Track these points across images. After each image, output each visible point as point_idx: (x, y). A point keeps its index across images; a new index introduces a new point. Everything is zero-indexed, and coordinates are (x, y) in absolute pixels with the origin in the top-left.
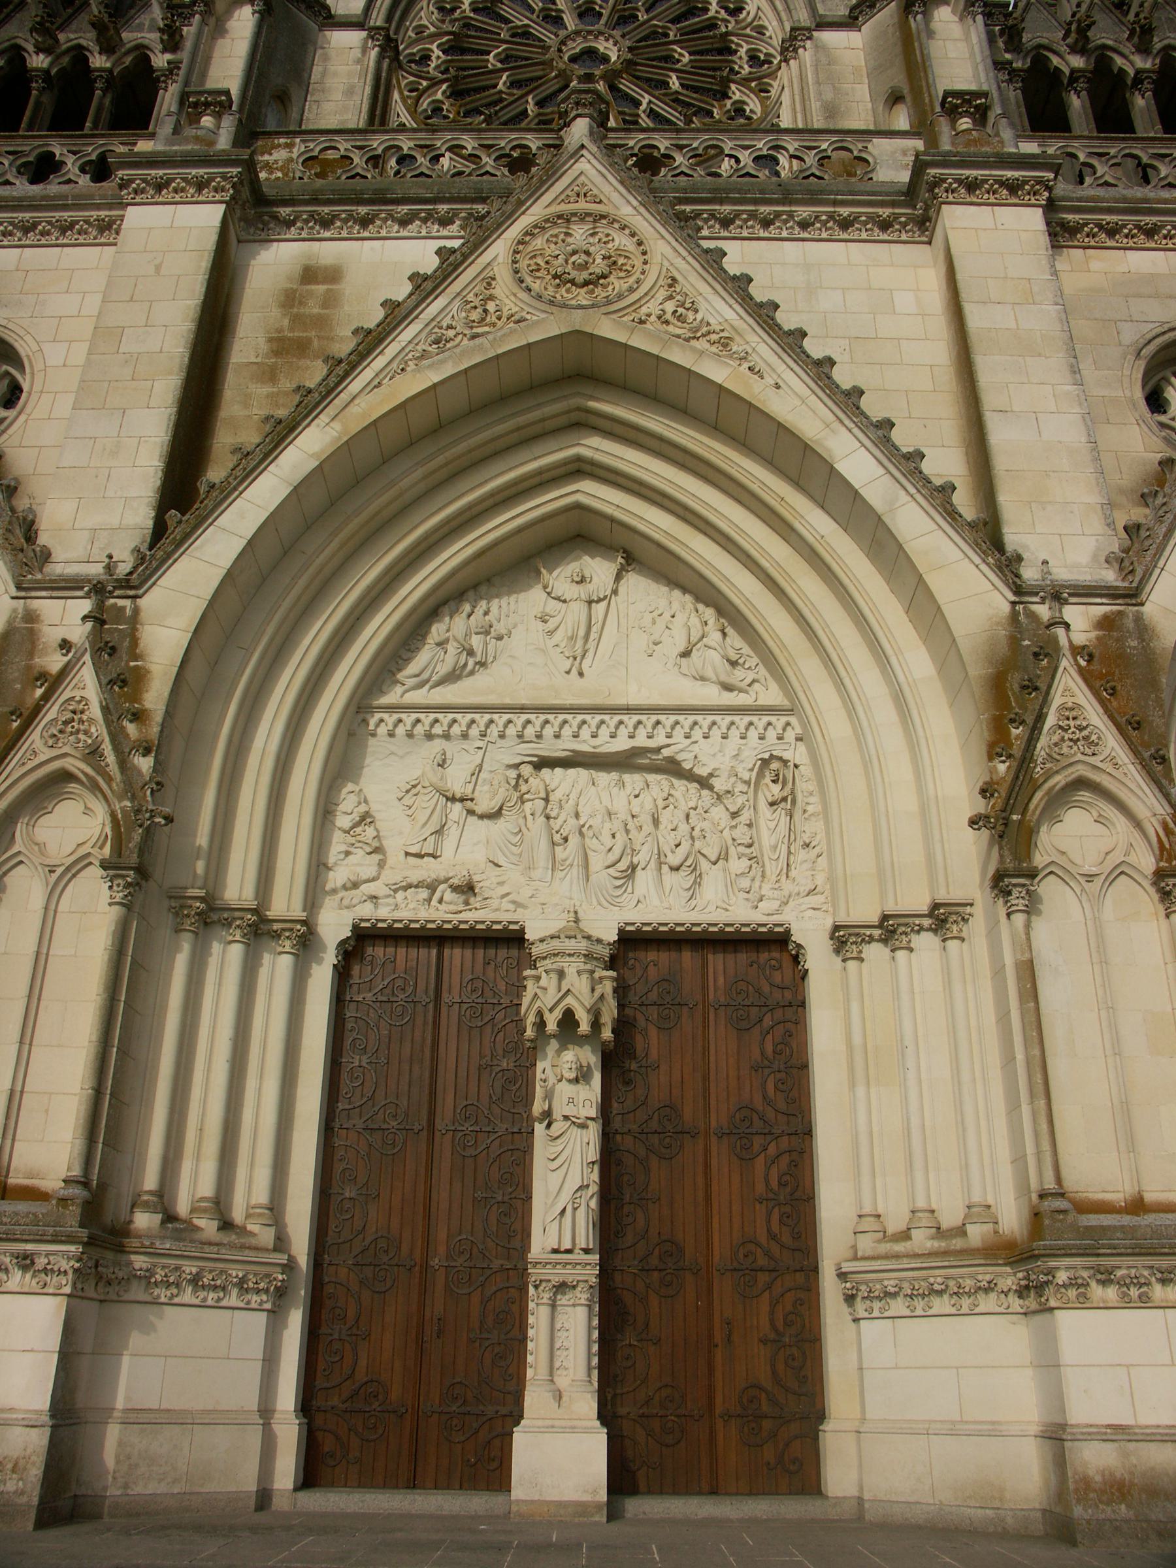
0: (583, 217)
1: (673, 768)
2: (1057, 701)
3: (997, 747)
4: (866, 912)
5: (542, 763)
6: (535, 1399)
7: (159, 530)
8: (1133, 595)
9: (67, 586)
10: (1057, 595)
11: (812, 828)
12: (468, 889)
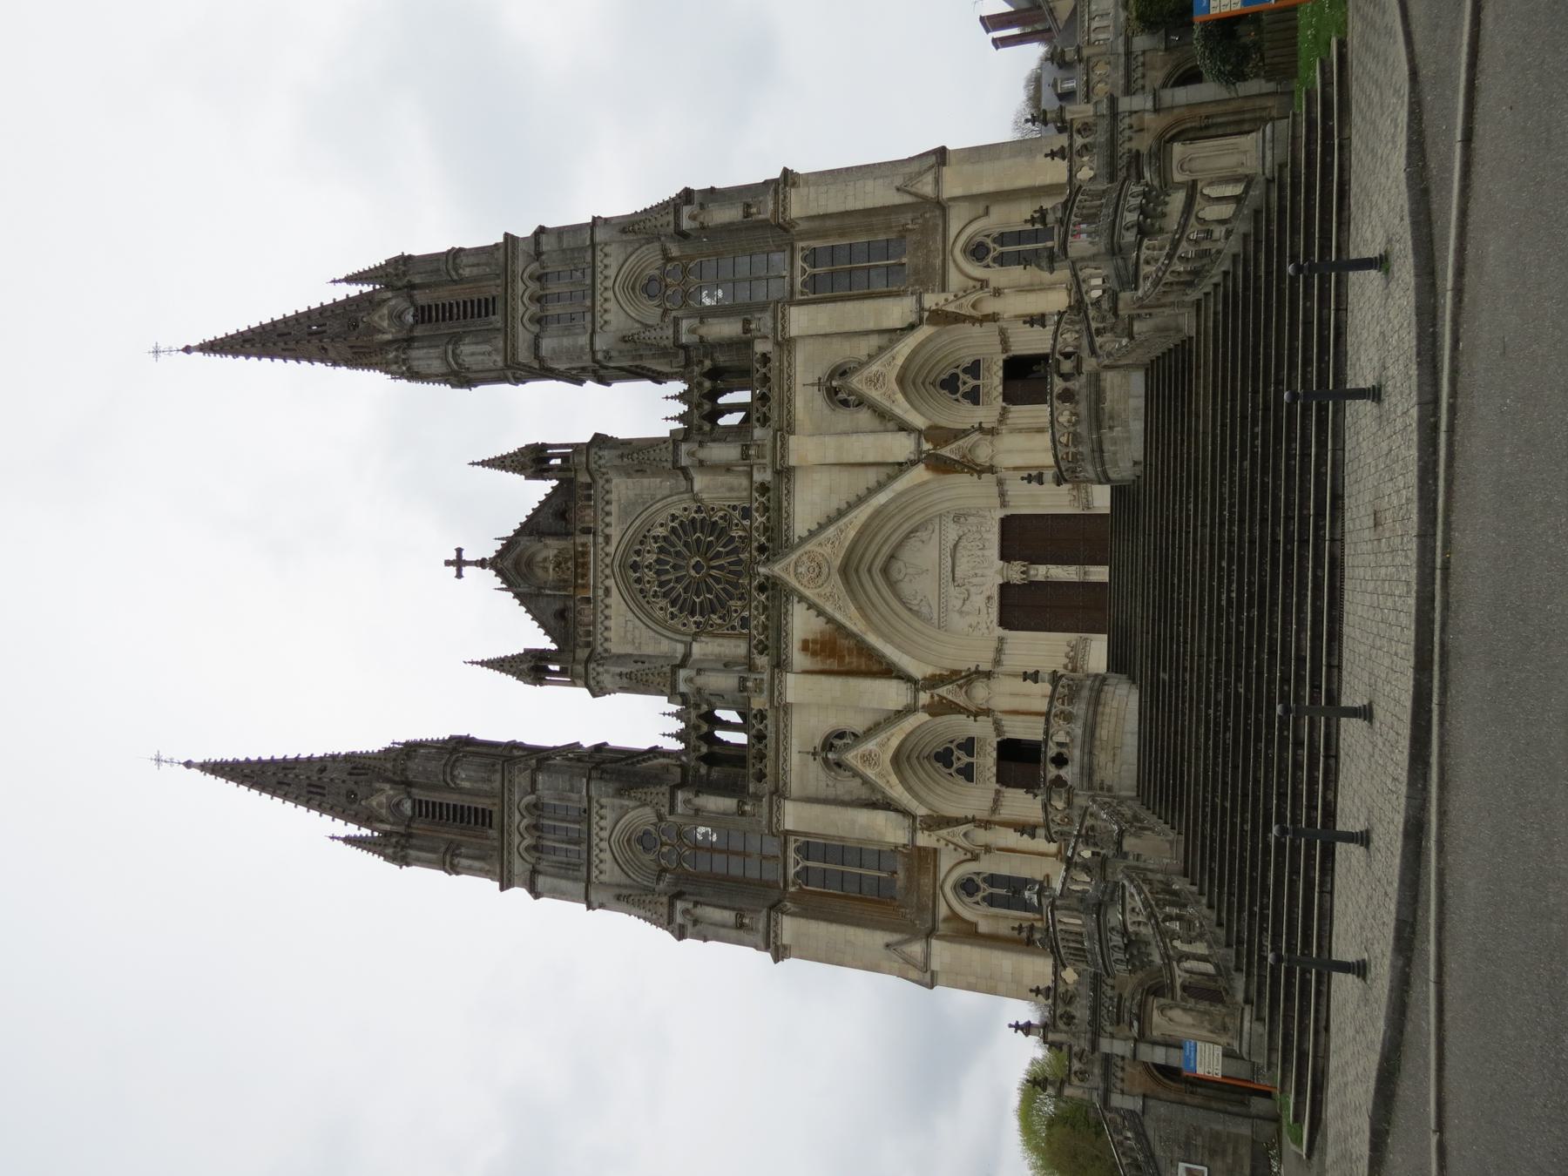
0: (795, 570)
1: (955, 546)
2: (948, 455)
4: (997, 501)
5: (953, 580)
8: (920, 432)
9: (916, 698)
10: (921, 452)
11: (974, 512)
12: (989, 598)
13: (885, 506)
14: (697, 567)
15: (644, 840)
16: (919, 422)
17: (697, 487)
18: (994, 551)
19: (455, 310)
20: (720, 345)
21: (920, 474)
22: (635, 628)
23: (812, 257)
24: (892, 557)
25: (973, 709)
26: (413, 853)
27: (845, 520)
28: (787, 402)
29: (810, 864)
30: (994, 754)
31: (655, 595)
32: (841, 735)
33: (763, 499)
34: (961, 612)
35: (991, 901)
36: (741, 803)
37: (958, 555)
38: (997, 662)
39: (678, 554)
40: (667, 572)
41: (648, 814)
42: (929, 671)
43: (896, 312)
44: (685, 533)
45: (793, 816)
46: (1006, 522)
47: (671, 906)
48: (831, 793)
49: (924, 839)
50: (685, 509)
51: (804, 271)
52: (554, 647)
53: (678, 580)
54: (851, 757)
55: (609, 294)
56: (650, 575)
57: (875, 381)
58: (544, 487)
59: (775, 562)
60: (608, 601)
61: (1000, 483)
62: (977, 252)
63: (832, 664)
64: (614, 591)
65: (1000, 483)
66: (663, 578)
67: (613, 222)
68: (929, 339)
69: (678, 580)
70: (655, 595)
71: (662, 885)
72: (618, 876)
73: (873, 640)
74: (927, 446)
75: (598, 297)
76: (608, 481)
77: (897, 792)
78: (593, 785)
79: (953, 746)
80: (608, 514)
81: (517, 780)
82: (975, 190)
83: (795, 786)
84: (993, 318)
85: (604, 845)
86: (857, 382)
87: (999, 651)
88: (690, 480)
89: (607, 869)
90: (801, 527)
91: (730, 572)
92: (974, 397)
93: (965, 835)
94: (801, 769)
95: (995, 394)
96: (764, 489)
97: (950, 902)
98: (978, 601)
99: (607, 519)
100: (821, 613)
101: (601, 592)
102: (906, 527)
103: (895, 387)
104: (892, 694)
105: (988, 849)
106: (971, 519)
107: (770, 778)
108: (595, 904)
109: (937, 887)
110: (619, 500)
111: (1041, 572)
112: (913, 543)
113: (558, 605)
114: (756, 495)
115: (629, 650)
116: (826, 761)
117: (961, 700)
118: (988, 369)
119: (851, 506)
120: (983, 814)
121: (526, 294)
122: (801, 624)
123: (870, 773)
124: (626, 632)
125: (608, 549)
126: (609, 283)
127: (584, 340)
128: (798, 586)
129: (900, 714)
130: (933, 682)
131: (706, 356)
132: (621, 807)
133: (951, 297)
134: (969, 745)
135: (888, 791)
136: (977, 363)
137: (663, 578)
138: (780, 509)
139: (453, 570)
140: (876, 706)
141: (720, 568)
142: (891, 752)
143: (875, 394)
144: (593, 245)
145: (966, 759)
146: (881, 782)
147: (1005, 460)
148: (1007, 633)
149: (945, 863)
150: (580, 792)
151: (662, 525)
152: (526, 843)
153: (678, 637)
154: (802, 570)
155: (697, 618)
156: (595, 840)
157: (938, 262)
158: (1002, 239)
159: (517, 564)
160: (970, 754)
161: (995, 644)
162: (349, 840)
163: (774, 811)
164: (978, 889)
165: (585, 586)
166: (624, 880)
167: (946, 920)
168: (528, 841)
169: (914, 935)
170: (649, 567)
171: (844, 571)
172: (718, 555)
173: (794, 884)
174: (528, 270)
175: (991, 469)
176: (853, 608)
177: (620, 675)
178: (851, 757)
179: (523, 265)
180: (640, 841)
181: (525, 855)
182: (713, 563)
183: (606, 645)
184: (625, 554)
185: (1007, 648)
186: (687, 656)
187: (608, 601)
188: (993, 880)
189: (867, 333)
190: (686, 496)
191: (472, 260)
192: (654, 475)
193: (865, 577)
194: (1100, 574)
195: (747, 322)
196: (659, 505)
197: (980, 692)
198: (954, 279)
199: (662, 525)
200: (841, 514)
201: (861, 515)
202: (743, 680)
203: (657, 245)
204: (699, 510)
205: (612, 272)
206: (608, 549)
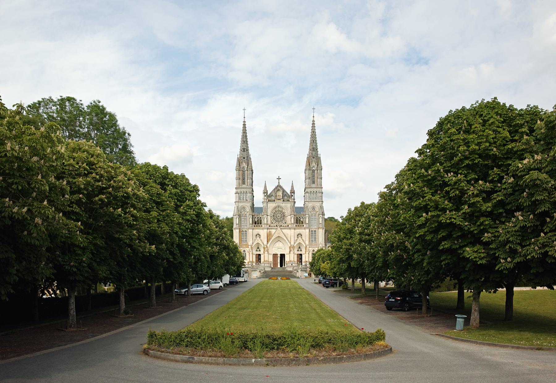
14: (279, 216)
16: (295, 245)
21: (290, 245)
23: (315, 231)
26: (238, 171)
28: (298, 229)
41: (248, 210)
43: (307, 243)
46: (284, 255)
49: (250, 247)
57: (300, 240)
58: (289, 193)
83: (254, 231)
84: (306, 253)
86: (300, 238)
89: (241, 205)
90: (283, 231)
94: (256, 231)
96: (288, 226)
98: (276, 251)
100: (274, 234)
104: (265, 243)
105: (250, 254)
113: (274, 196)
119: (286, 237)
122: (273, 231)
127: (307, 200)
130: (267, 247)
139: (278, 178)
149: (247, 249)
175: (290, 253)
178: (258, 238)
179: (318, 190)
188: (245, 254)
197: (266, 252)
198: (310, 249)
201: (285, 238)
205: (316, 204)
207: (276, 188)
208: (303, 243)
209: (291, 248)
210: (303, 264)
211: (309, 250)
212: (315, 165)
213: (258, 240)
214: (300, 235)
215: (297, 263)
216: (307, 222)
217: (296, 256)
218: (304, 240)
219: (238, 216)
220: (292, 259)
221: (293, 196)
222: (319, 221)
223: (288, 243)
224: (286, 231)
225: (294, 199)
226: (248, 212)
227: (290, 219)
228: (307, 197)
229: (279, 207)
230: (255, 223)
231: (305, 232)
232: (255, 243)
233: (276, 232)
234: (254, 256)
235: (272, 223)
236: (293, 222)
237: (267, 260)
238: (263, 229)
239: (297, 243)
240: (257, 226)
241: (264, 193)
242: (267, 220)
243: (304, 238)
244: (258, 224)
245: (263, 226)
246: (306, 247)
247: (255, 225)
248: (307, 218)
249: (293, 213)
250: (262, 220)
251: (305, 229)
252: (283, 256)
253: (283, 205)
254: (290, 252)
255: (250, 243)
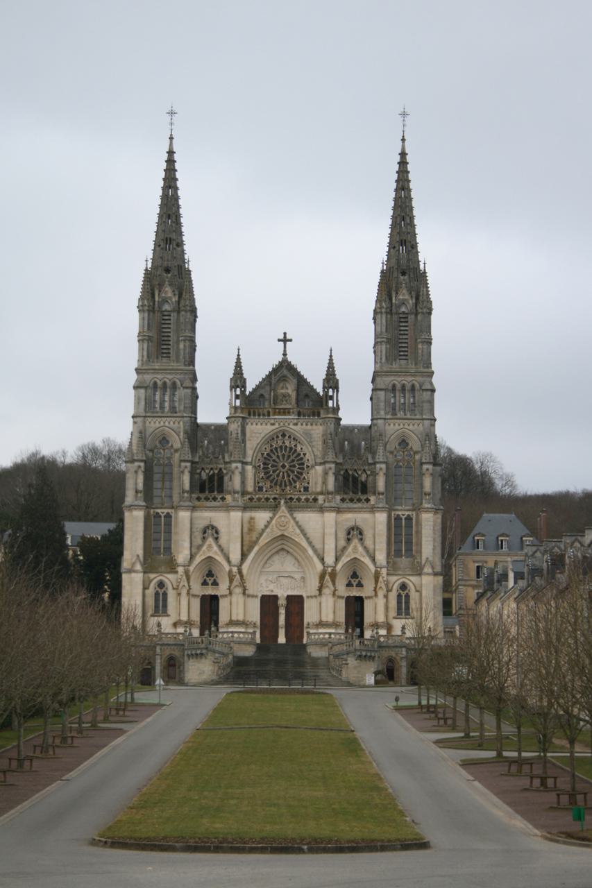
1: (293, 578)
3: (320, 583)
4: (309, 595)
6: (280, 636)
7: (242, 559)
10: (328, 567)
13: (307, 551)
15: (164, 440)
17: (317, 468)
18: (291, 593)
19: (404, 337)
20: (375, 480)
21: (319, 567)
22: (258, 438)
23: (409, 519)
24: (288, 552)
25: (232, 588)
26: (146, 315)
27: (302, 537)
28: (350, 510)
29: (163, 519)
30: (213, 594)
31: (272, 446)
32: (217, 532)
33: (311, 500)
34: (267, 580)
35: (157, 594)
36: (187, 492)
37: (289, 578)
38: (249, 596)
39: (289, 457)
40: (281, 451)
42: (245, 571)
43: (381, 557)
44: (298, 460)
45: (184, 516)
47: (142, 461)
48: (194, 530)
49: (181, 570)
50: (308, 460)
51: (403, 515)
52: (247, 393)
53: (278, 457)
54: (210, 541)
55: (402, 426)
56: (280, 443)
57: (355, 549)
59: (286, 507)
60: (269, 424)
61: (316, 596)
62: (403, 587)
63: (245, 530)
64: (274, 427)
65: (316, 596)
66: (279, 450)
67: (432, 428)
68: (370, 570)
69: (278, 457)
70: (272, 446)
71: (148, 452)
72: (150, 431)
73: (256, 548)
74: (330, 570)
75: (400, 421)
76: (321, 425)
77: (198, 559)
78: (189, 419)
79: (215, 577)
80: (307, 425)
81: (187, 377)
82: (423, 588)
83: (197, 514)
84: (376, 595)
85: (162, 424)
86: (355, 542)
87: (253, 596)
88: (321, 464)
89: (154, 425)
90: (301, 516)
91: (281, 482)
92: (349, 585)
93: (184, 586)
95: (350, 593)
96: (315, 500)
97: (155, 578)
98: (271, 587)
99: (304, 424)
100: (266, 527)
101: (272, 421)
102: (299, 558)
103: (352, 557)
104: (235, 556)
105: (179, 594)
106: (302, 584)
107: (197, 503)
108: (135, 419)
109: (161, 573)
110: (312, 430)
111: (282, 611)
112: (293, 561)
113: (267, 396)
114: (313, 497)
115: (248, 435)
116: (208, 527)
117: (235, 583)
118: (360, 591)
119: (307, 539)
120: (191, 592)
121: (406, 382)
122: (262, 517)
123: (204, 548)
124: (256, 433)
125: (291, 424)
126: (406, 426)
128: (277, 517)
129: (229, 561)
130: (240, 572)
131: (371, 472)
132: (180, 432)
133: (385, 579)
134: (215, 584)
135: (198, 556)
136: (362, 586)
137: (279, 450)
138: (307, 508)
140: (231, 549)
141: (283, 477)
142: (213, 556)
143: (350, 549)
144: (423, 419)
145: (210, 583)
146: (201, 552)
147: (324, 599)
148: (259, 598)
149: (170, 576)
150: (184, 412)
151: (302, 449)
152: (158, 381)
153: (254, 458)
154: (283, 519)
155: (262, 466)
156: (164, 419)
157: (400, 573)
158: (407, 596)
159: (285, 376)
160: (212, 584)
161: (255, 594)
162: (146, 270)
163: (186, 508)
164: (161, 588)
165: (274, 414)
166: (148, 434)
167: (149, 577)
168: (159, 383)
169: (144, 564)
170: (284, 443)
171: (283, 535)
172: (289, 476)
173: (154, 512)
174: (416, 383)
175: (320, 594)
176: (268, 540)
177: (238, 434)
178: (210, 541)
179: (417, 380)
180: (164, 438)
181: (153, 381)
182: (285, 474)
183: (250, 424)
184: (288, 431)
185: (254, 599)
186: (246, 463)
187: (269, 424)
188: (165, 594)
189: (375, 545)
190: (314, 462)
191: (425, 350)
192: (323, 448)
193: (280, 542)
194: (282, 639)
195: (383, 494)
196: (310, 449)
197: (238, 590)
198: (393, 579)
199: (302, 449)
200: (305, 535)
201: (304, 543)
202: (238, 493)
203: (420, 449)
204: (308, 467)
205: (411, 427)
206: (291, 424)
207: (275, 371)
208: (367, 561)
209: (327, 576)
210: (368, 634)
211: (387, 585)
212: (407, 297)
213: (210, 549)
214: (355, 532)
215: (347, 631)
216: (381, 484)
217: (342, 604)
218: (371, 547)
219: (142, 464)
220: (328, 616)
221: (331, 398)
222: (422, 486)
223: (316, 560)
224: (310, 520)
225: (336, 409)
226: (176, 451)
227: (320, 477)
228: (382, 405)
229: (284, 435)
230: (202, 490)
231: (377, 523)
232: (198, 559)
233: (272, 519)
234: (196, 604)
235: (261, 489)
236: (331, 485)
237: (241, 618)
238: (228, 508)
239: (344, 560)
240: (207, 499)
241: (232, 388)
242: (242, 476)
243: (369, 542)
244: (211, 491)
245: (229, 498)
246: (377, 576)
247: (202, 496)
248: (381, 474)
249: (331, 457)
250: (226, 479)
251: (373, 510)
252: (296, 603)
253: (298, 427)
254: (320, 589)
255: (182, 555)
